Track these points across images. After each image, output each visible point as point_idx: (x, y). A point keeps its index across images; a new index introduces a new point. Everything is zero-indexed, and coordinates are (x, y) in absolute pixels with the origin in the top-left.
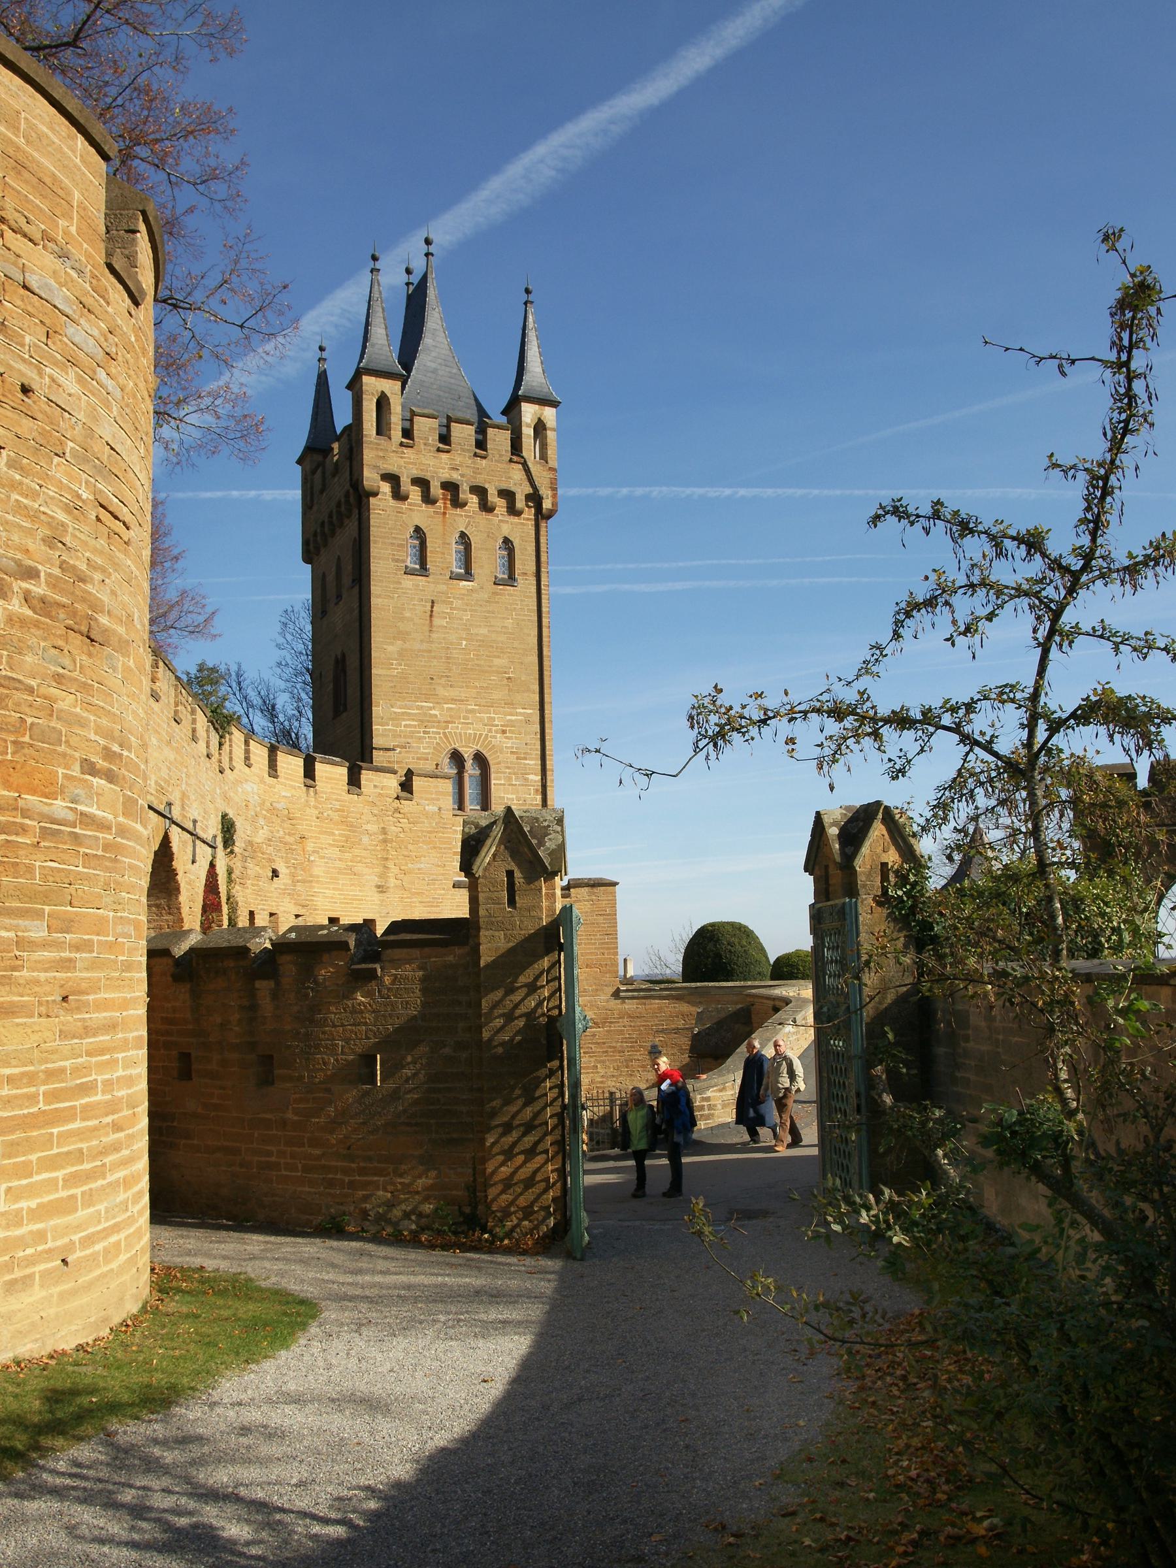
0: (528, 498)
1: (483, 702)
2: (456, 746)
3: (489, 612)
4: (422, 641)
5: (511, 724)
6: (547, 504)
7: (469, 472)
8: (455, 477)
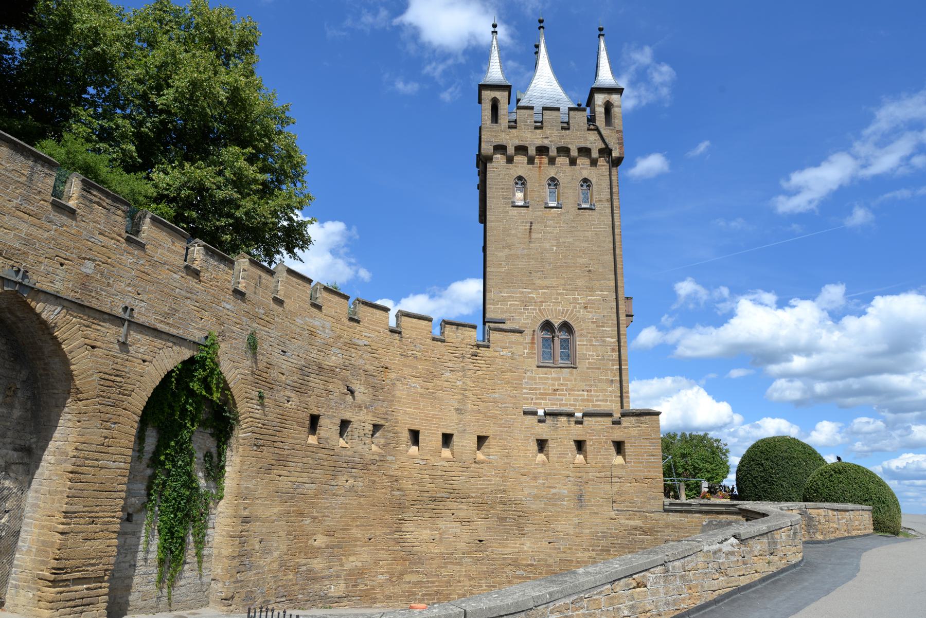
0: (601, 151)
1: (569, 287)
2: (549, 318)
3: (573, 227)
4: (523, 249)
5: (591, 302)
6: (615, 154)
7: (556, 139)
8: (546, 142)
